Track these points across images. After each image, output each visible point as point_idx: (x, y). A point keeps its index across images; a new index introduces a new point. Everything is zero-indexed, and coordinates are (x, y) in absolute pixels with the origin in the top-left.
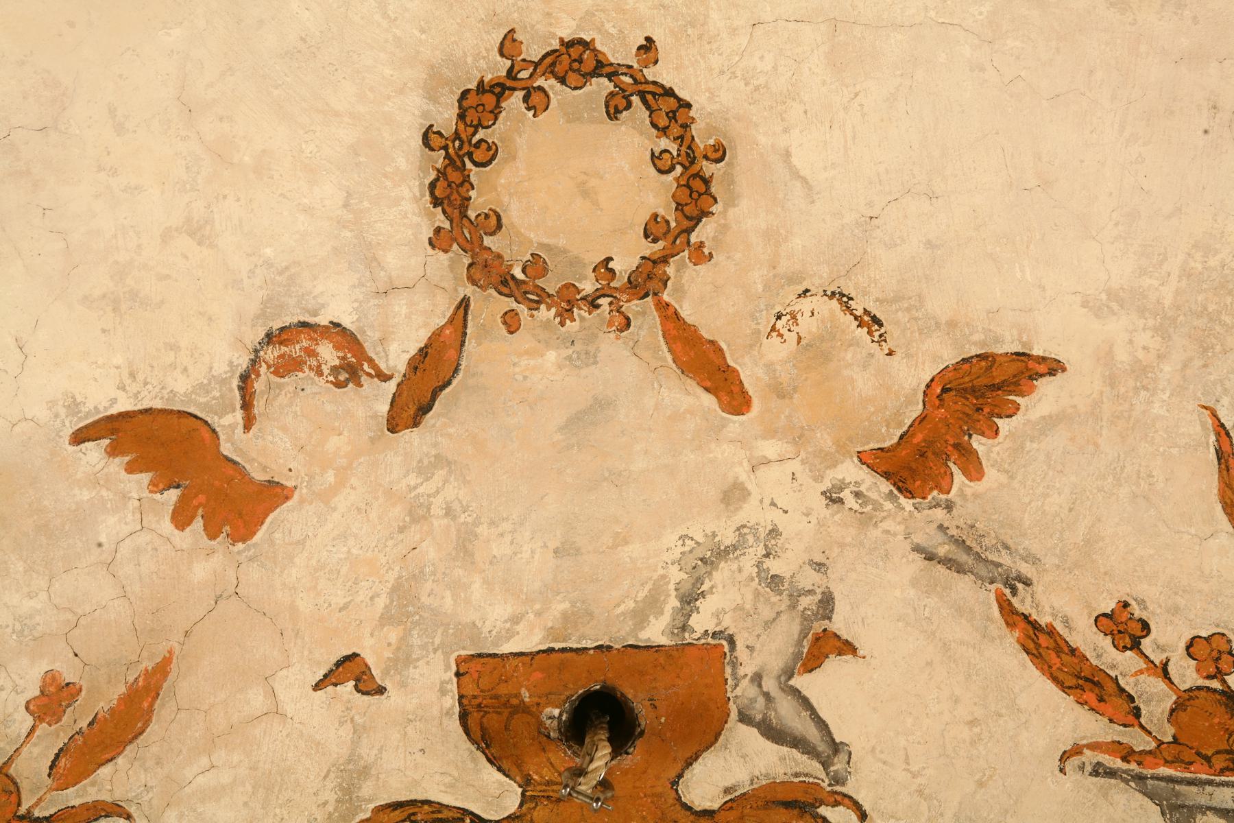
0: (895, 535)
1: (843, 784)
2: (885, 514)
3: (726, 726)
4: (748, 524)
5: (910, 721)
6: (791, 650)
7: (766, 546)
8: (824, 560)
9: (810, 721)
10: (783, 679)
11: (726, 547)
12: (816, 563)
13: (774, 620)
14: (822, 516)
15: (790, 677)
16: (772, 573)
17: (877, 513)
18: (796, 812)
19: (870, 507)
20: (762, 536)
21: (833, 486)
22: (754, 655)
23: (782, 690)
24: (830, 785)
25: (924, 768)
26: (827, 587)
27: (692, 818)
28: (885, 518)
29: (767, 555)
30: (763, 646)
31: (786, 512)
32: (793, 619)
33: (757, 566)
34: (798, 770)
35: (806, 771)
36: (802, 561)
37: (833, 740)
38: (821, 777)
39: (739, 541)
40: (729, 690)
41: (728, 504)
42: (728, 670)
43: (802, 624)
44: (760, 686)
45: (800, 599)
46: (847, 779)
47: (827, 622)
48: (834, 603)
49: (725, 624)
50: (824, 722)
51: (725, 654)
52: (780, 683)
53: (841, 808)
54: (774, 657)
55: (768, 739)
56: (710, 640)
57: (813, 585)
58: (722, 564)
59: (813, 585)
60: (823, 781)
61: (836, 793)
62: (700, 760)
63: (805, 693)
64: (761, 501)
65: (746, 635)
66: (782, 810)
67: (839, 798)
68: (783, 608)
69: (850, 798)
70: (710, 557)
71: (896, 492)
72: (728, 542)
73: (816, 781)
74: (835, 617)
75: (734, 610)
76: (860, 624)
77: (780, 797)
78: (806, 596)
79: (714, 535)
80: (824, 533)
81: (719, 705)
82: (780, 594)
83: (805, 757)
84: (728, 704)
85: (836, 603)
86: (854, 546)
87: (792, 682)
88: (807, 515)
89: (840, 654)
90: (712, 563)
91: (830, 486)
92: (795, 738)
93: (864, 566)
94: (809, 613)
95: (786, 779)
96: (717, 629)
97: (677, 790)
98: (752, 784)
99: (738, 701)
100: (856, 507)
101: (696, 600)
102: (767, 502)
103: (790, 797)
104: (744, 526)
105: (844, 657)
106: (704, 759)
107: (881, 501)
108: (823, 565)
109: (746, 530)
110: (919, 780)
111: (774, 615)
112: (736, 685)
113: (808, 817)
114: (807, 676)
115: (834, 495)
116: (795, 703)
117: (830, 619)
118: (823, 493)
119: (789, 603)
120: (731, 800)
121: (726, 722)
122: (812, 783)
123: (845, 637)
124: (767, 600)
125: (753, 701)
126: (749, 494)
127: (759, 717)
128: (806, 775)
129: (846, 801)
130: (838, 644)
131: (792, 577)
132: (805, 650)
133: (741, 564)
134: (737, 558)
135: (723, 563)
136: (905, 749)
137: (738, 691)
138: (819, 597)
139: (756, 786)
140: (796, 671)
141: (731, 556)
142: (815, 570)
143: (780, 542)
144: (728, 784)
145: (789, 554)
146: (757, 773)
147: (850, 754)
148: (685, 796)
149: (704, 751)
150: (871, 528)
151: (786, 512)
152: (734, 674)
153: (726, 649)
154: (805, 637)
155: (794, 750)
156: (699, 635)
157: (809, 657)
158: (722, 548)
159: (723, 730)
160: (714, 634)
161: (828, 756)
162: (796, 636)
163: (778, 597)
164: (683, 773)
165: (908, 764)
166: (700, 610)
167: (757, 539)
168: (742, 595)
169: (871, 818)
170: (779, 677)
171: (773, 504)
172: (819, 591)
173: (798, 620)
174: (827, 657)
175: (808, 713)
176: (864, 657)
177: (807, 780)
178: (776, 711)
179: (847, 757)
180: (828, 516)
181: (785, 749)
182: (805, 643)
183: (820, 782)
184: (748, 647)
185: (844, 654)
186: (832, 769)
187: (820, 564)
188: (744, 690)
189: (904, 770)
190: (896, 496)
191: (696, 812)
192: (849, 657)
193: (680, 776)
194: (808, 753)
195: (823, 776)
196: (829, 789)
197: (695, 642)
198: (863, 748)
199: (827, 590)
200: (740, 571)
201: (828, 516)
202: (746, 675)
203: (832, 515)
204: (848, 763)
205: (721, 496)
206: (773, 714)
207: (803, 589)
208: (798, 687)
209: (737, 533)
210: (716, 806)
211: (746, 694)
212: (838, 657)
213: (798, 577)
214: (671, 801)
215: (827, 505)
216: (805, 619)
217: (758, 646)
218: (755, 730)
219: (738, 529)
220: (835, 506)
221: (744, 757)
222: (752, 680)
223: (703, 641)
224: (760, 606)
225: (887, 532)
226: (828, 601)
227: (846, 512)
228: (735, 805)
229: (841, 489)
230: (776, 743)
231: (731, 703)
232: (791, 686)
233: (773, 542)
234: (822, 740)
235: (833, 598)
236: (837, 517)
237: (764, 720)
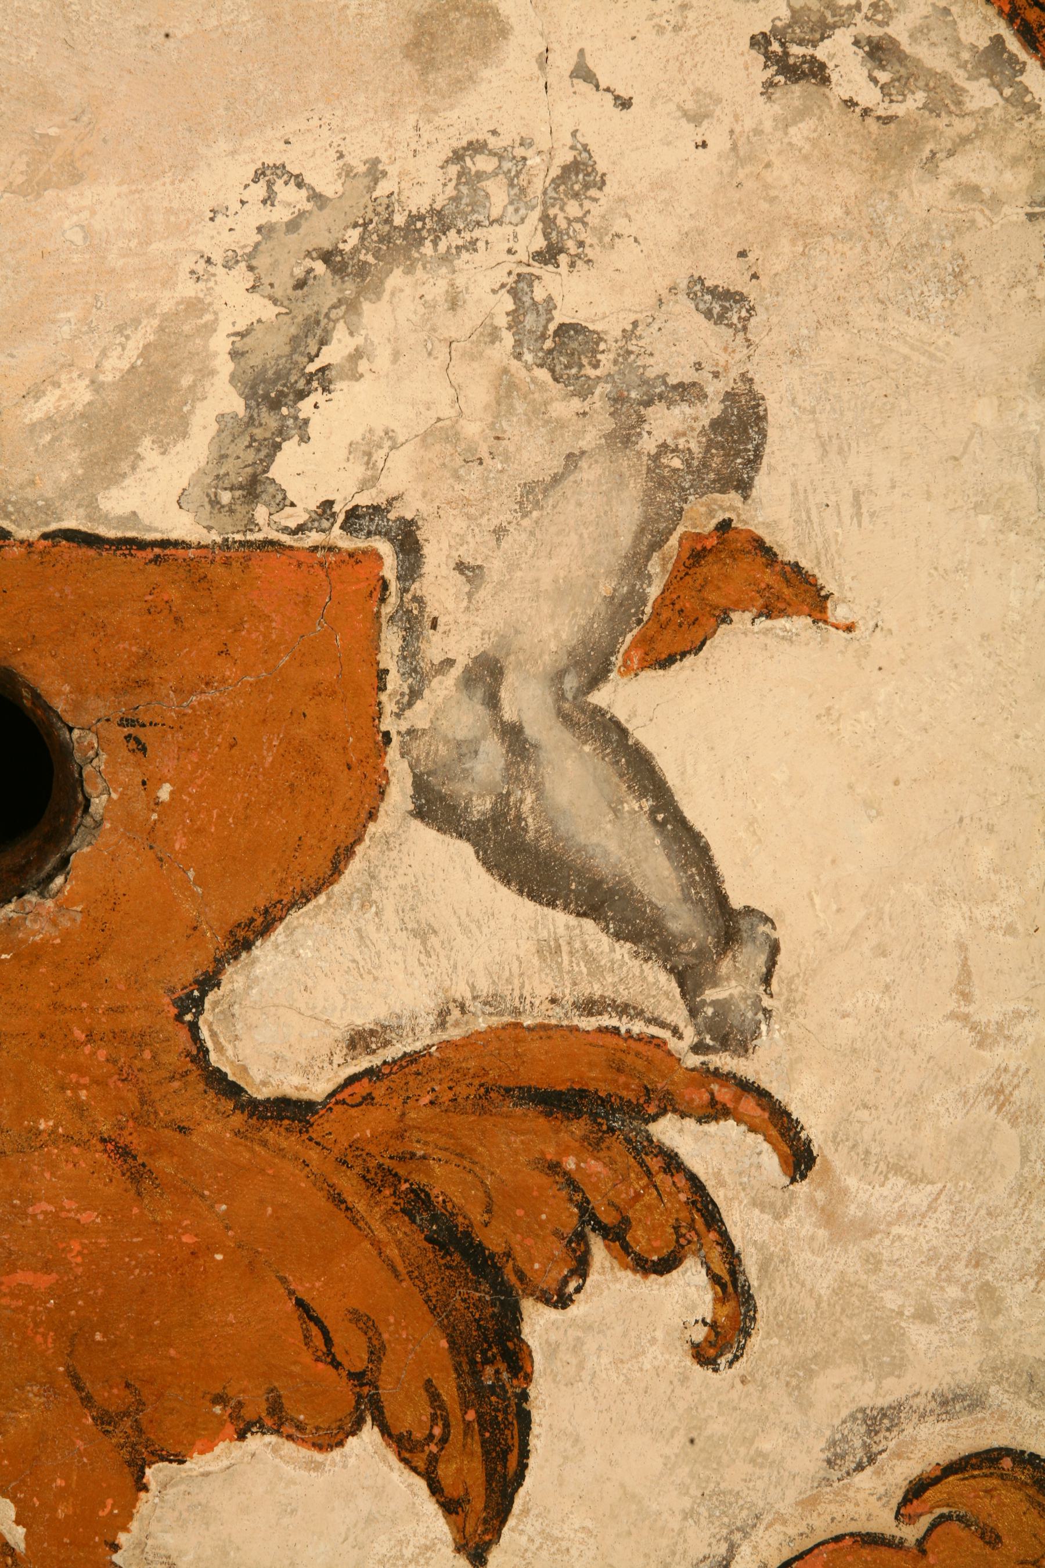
0: (996, 202)
1: (743, 1048)
2: (965, 126)
3: (372, 828)
4: (493, 142)
5: (985, 853)
6: (606, 587)
7: (547, 221)
8: (740, 283)
9: (649, 831)
10: (571, 683)
11: (413, 218)
12: (713, 291)
13: (556, 480)
14: (749, 124)
15: (597, 679)
16: (560, 317)
17: (941, 123)
18: (579, 1127)
19: (913, 102)
20: (538, 186)
21: (797, 16)
22: (483, 594)
23: (566, 718)
24: (698, 1048)
25: (1019, 1016)
26: (746, 379)
27: (238, 1120)
28: (965, 140)
29: (549, 255)
30: (512, 567)
31: (625, 104)
32: (620, 482)
33: (514, 292)
34: (597, 990)
35: (624, 996)
36: (667, 282)
37: (722, 900)
38: (671, 1019)
39: (456, 199)
40: (390, 707)
41: (428, 66)
42: (391, 640)
43: (648, 500)
44: (493, 701)
45: (649, 412)
46: (756, 1034)
47: (733, 497)
48: (763, 434)
49: (388, 486)
50: (695, 837)
51: (385, 586)
52: (561, 697)
53: (729, 1127)
54: (546, 608)
55: (506, 880)
56: (338, 537)
57: (698, 366)
58: (396, 279)
59: (698, 366)
60: (676, 1032)
61: (716, 1073)
62: (279, 934)
63: (642, 735)
64: (543, 60)
65: (459, 525)
66: (533, 1119)
67: (724, 1094)
68: (590, 439)
69: (762, 1095)
70: (355, 250)
71: (1013, 44)
72: (419, 201)
73: (654, 1030)
74: (762, 482)
75: (425, 438)
76: (847, 510)
77: (533, 1077)
78: (671, 403)
79: (375, 172)
80: (750, 185)
81: (354, 759)
82: (584, 393)
83: (623, 950)
84: (381, 754)
85: (772, 433)
86: (851, 236)
87: (599, 698)
88: (696, 119)
89: (768, 612)
90: (363, 269)
91: (785, 14)
92: (596, 885)
93: (876, 309)
94: (677, 463)
95: (556, 1016)
96: (364, 500)
97: (194, 1028)
98: (442, 1025)
99: (419, 748)
100: (869, 96)
101: (302, 395)
102: (563, 62)
103: (562, 1080)
104: (476, 147)
105: (782, 622)
106: (291, 932)
107: (960, 78)
108: (738, 298)
109: (483, 163)
110: (1000, 1054)
111: (557, 465)
112: (415, 694)
113: (616, 1146)
114: (652, 680)
115: (795, 50)
116: (605, 768)
117: (744, 487)
118: (759, 42)
119: (610, 425)
120: (369, 1072)
121: (372, 816)
122: (640, 1038)
123: (790, 553)
124: (539, 411)
125: (466, 749)
126: (504, 32)
127: (481, 806)
128: (624, 1010)
129: (749, 1105)
130: (768, 577)
131: (627, 335)
132: (654, 592)
133: (460, 281)
134: (446, 259)
135: (398, 272)
136: (962, 947)
137: (419, 715)
138: (715, 409)
139: (454, 1034)
140: (618, 660)
141: (428, 249)
142: (708, 314)
143: (596, 210)
144: (364, 1020)
145: (626, 255)
146: (461, 990)
147: (775, 949)
148: (220, 1049)
149: (293, 905)
150: (914, 174)
151: (625, 104)
152: (409, 655)
153: (389, 570)
154: (656, 545)
155: (588, 924)
156: (301, 517)
157: (666, 614)
158: (399, 220)
159: (359, 840)
160: (353, 514)
161: (701, 953)
162: (625, 541)
163: (576, 404)
164: (219, 971)
165: (966, 997)
166: (312, 430)
167: (520, 194)
168: (457, 388)
169: (827, 1169)
170: (559, 676)
171: (583, 73)
172: (715, 389)
173: (635, 487)
174: (725, 619)
175: (647, 804)
176: (849, 628)
177: (624, 1025)
178: (538, 788)
179: (762, 959)
180: (768, 125)
181: (560, 920)
182: (654, 567)
183: (665, 1034)
184: (461, 567)
185: (782, 613)
186: (711, 994)
187: (729, 297)
188: (439, 713)
189: (953, 1016)
190: (1013, 59)
191: (254, 1103)
192: (799, 623)
193: (209, 981)
194: (634, 937)
195: (677, 1014)
196: (693, 1061)
197: (286, 539)
198: (821, 934)
199: (742, 387)
200: (454, 303)
201: (768, 125)
202: (450, 662)
203: (785, 124)
204: (767, 979)
205: (408, 33)
206: (530, 798)
207: (663, 378)
208: (621, 714)
209: (453, 170)
210: (318, 1089)
211: (444, 724)
212: (763, 623)
213: (648, 337)
214: (172, 1059)
215: (770, 84)
216: (662, 484)
217: (495, 568)
218: (466, 849)
219: (457, 156)
220: (797, 89)
221: (423, 933)
222: (468, 681)
223: (314, 538)
224: (512, 428)
225: (969, 191)
226: (743, 427)
227: (833, 114)
228: (380, 1090)
229: (823, 30)
230: (533, 896)
231: (393, 751)
232: (598, 711)
233: (573, 209)
234: (687, 898)
235: (764, 418)
236: (800, 133)
237: (497, 818)
